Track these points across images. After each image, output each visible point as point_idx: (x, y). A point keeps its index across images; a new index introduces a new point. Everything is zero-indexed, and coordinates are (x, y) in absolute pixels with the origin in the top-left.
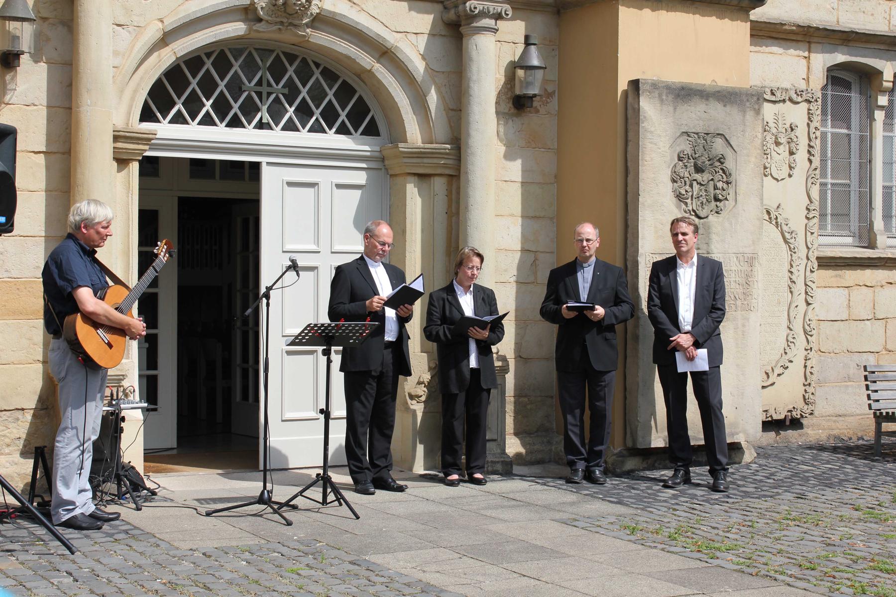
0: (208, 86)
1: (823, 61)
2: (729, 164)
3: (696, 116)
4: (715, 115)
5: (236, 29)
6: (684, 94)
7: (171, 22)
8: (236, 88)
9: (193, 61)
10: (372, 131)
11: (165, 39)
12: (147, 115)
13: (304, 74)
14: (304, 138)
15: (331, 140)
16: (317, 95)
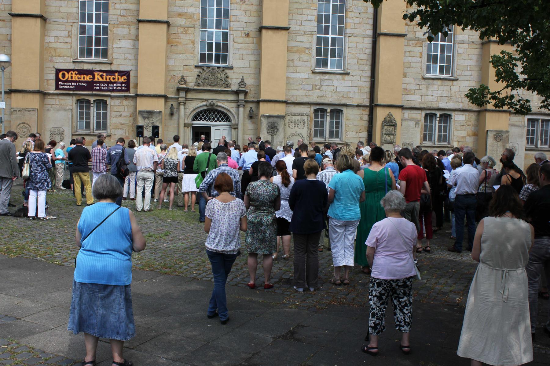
0: (203, 116)
1: (313, 108)
2: (278, 127)
3: (271, 120)
4: (275, 120)
5: (205, 108)
6: (269, 117)
7: (195, 108)
8: (207, 116)
9: (201, 112)
10: (229, 121)
11: (194, 110)
12: (194, 120)
13: (218, 113)
14: (218, 123)
15: (222, 123)
16: (220, 116)
